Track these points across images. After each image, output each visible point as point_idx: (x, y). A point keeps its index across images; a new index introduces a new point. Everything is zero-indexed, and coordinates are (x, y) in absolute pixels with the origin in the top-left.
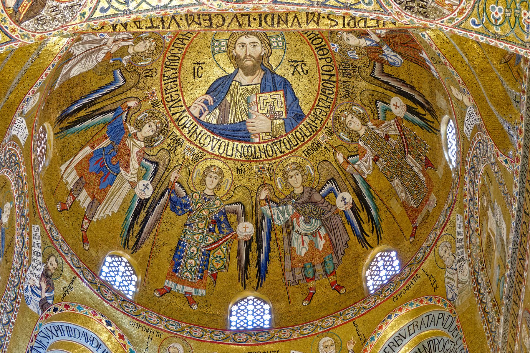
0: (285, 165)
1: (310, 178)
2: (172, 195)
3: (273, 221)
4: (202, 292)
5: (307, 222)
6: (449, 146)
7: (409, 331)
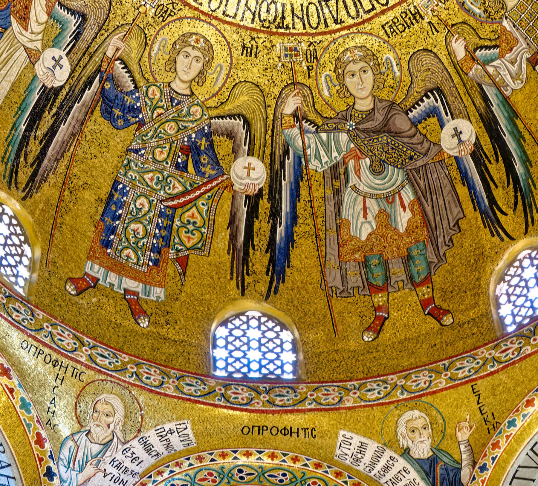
0: (341, 50)
1: (390, 82)
2: (108, 86)
4: (158, 293)
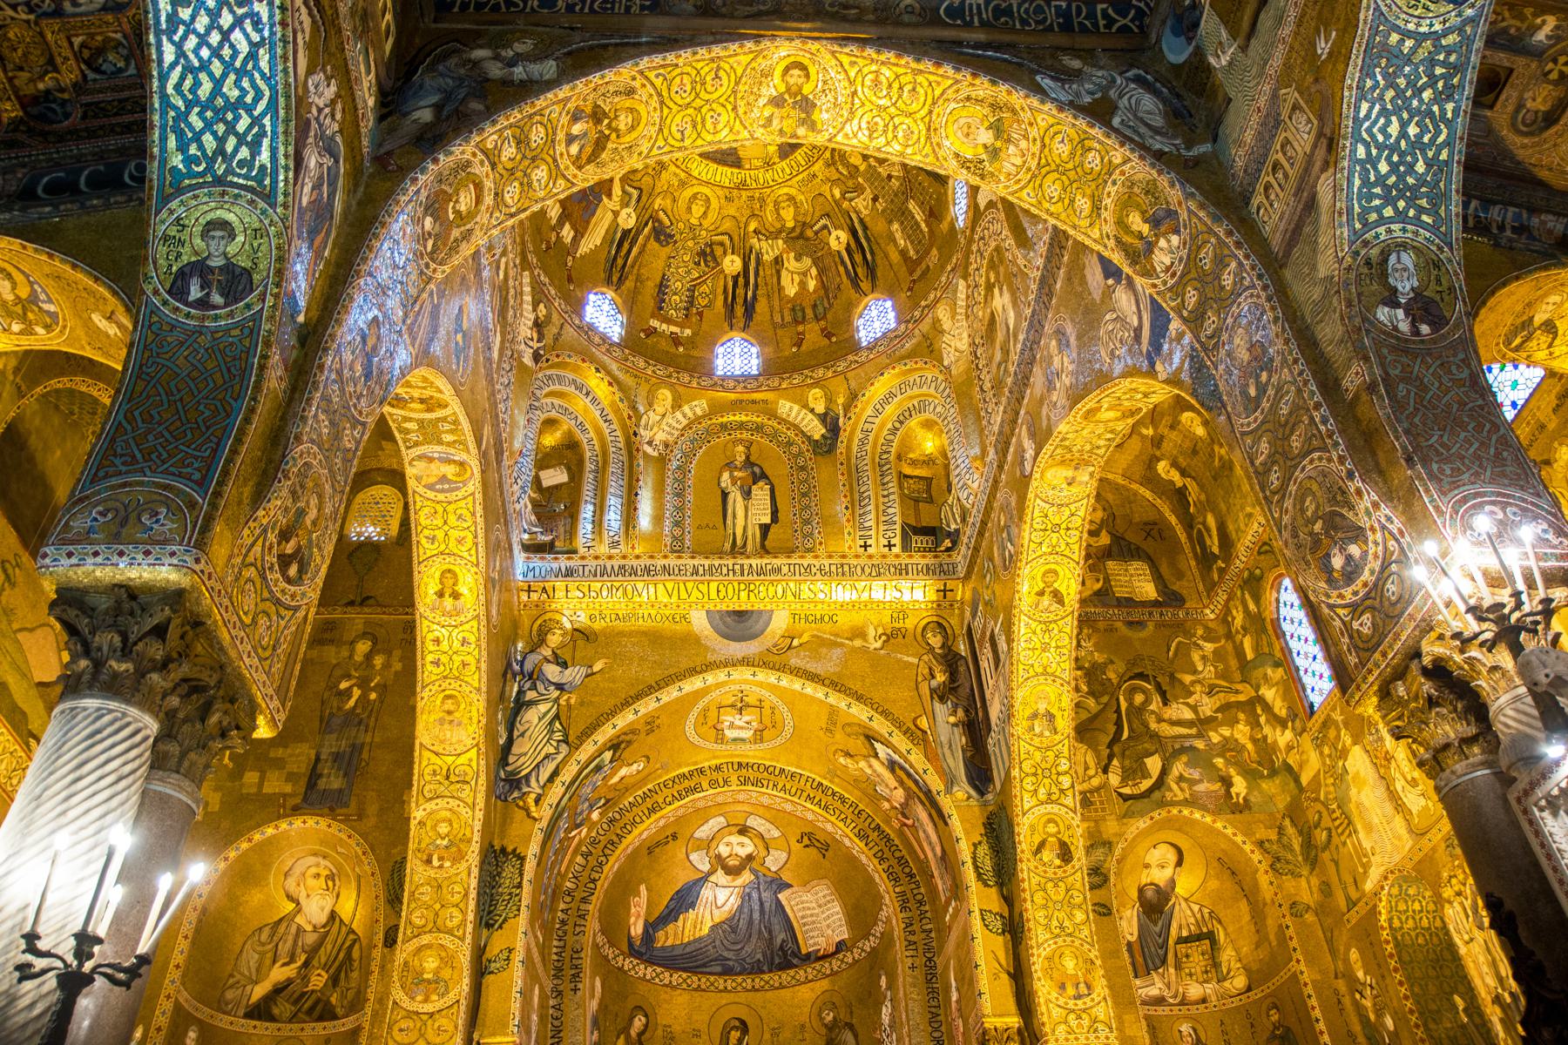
4: (688, 332)
5: (798, 259)
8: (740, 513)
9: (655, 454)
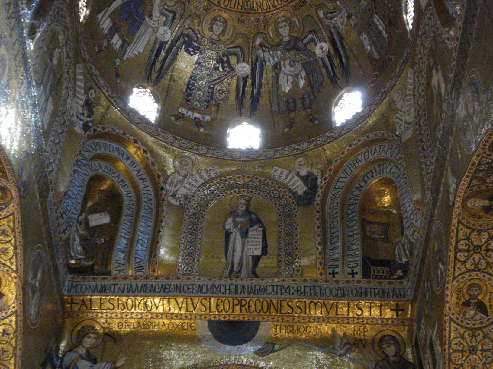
0: (276, 18)
2: (186, 39)
3: (265, 63)
4: (208, 118)
6: (408, 11)
7: (365, 156)
8: (238, 248)
9: (177, 204)
